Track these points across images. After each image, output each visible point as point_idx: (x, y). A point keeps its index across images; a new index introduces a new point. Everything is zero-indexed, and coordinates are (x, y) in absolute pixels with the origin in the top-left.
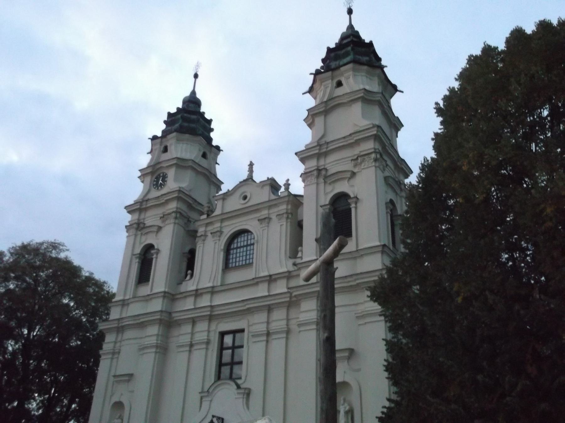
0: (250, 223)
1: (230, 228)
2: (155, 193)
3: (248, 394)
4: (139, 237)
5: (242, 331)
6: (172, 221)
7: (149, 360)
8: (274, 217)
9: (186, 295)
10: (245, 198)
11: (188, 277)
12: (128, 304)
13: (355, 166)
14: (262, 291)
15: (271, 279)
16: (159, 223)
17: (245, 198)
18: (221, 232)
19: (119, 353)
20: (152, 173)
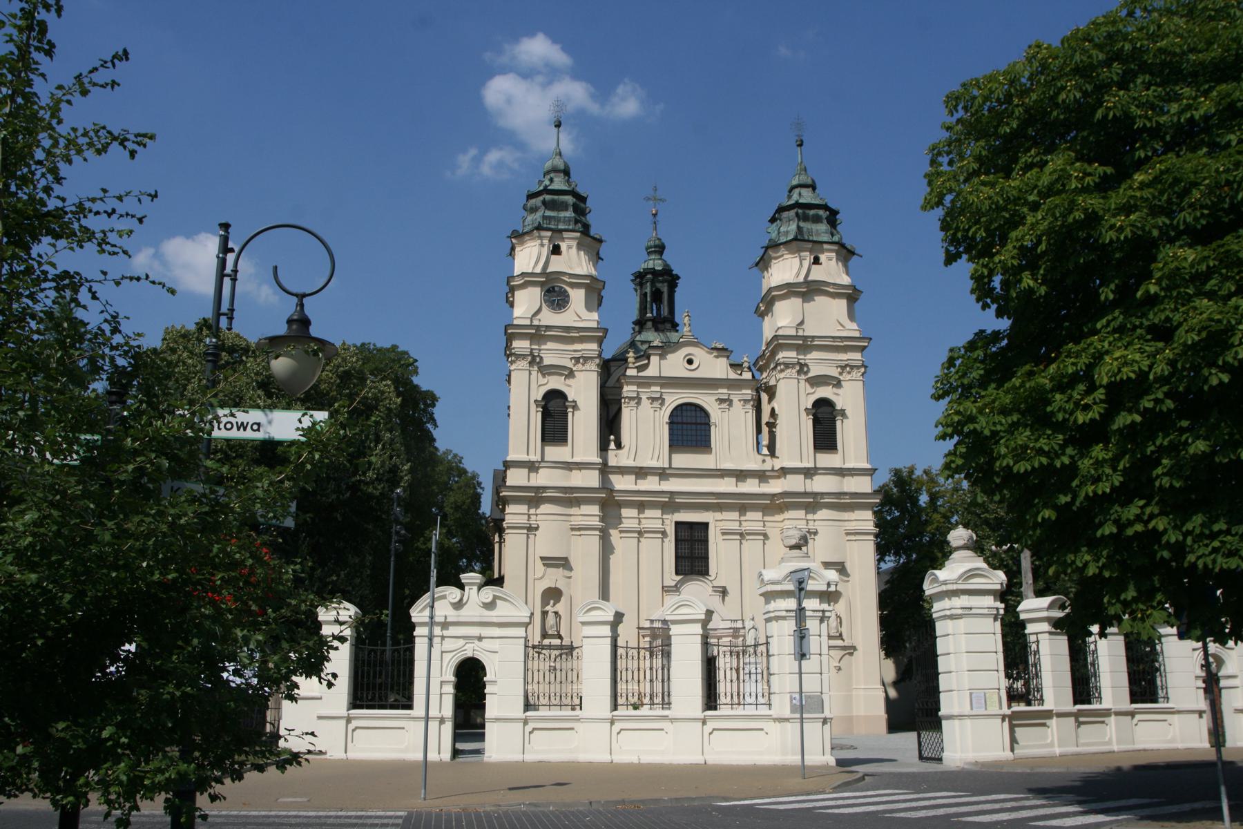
0: (706, 400)
1: (675, 398)
2: (549, 318)
3: (724, 592)
4: (534, 373)
5: (706, 525)
6: (594, 367)
7: (592, 543)
8: (735, 399)
9: (623, 471)
10: (690, 362)
11: (612, 446)
12: (538, 468)
13: (841, 374)
14: (727, 486)
15: (741, 475)
16: (570, 364)
17: (690, 362)
18: (663, 400)
19: (537, 529)
20: (541, 284)
